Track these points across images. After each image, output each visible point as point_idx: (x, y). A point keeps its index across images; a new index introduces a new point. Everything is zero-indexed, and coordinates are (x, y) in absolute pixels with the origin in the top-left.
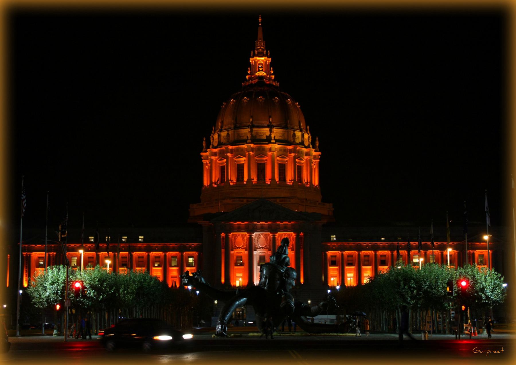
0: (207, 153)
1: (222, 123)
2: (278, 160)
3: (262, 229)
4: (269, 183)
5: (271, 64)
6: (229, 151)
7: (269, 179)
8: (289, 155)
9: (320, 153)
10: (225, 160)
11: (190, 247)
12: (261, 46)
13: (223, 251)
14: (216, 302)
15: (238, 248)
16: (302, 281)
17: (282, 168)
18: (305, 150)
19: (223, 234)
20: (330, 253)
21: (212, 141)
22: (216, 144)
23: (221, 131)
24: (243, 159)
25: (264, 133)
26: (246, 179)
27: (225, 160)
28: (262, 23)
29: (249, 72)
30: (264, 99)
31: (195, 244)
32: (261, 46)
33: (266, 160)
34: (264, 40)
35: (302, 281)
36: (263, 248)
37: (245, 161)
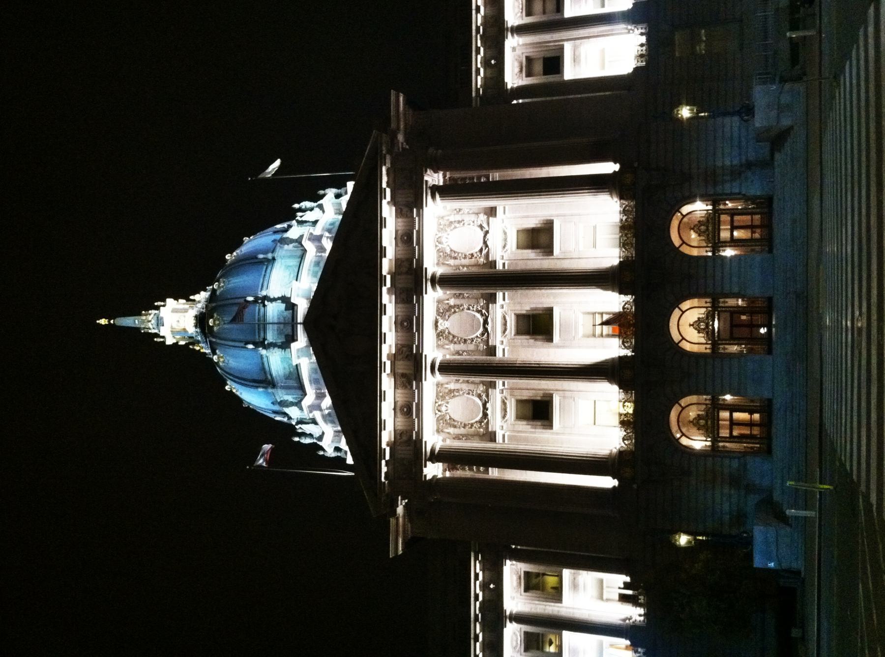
3: (410, 324)
5: (188, 300)
6: (318, 402)
11: (484, 586)
12: (147, 322)
13: (494, 473)
14: (683, 540)
15: (485, 415)
16: (609, 168)
19: (433, 470)
20: (513, 78)
21: (307, 441)
23: (290, 418)
25: (280, 314)
29: (197, 348)
30: (215, 315)
31: (476, 568)
32: (147, 322)
34: (140, 314)
35: (609, 168)
36: (486, 322)
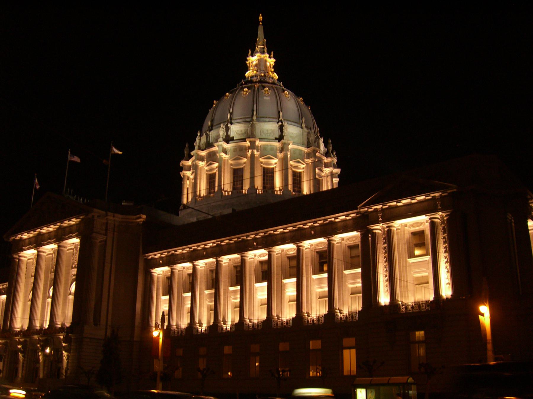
0: (189, 163)
1: (212, 121)
2: (291, 165)
4: (280, 193)
7: (280, 190)
8: (306, 160)
9: (337, 171)
10: (216, 165)
17: (297, 178)
18: (326, 160)
22: (203, 147)
24: (245, 160)
26: (246, 186)
27: (216, 165)
28: (262, 22)
33: (276, 164)
37: (245, 163)
